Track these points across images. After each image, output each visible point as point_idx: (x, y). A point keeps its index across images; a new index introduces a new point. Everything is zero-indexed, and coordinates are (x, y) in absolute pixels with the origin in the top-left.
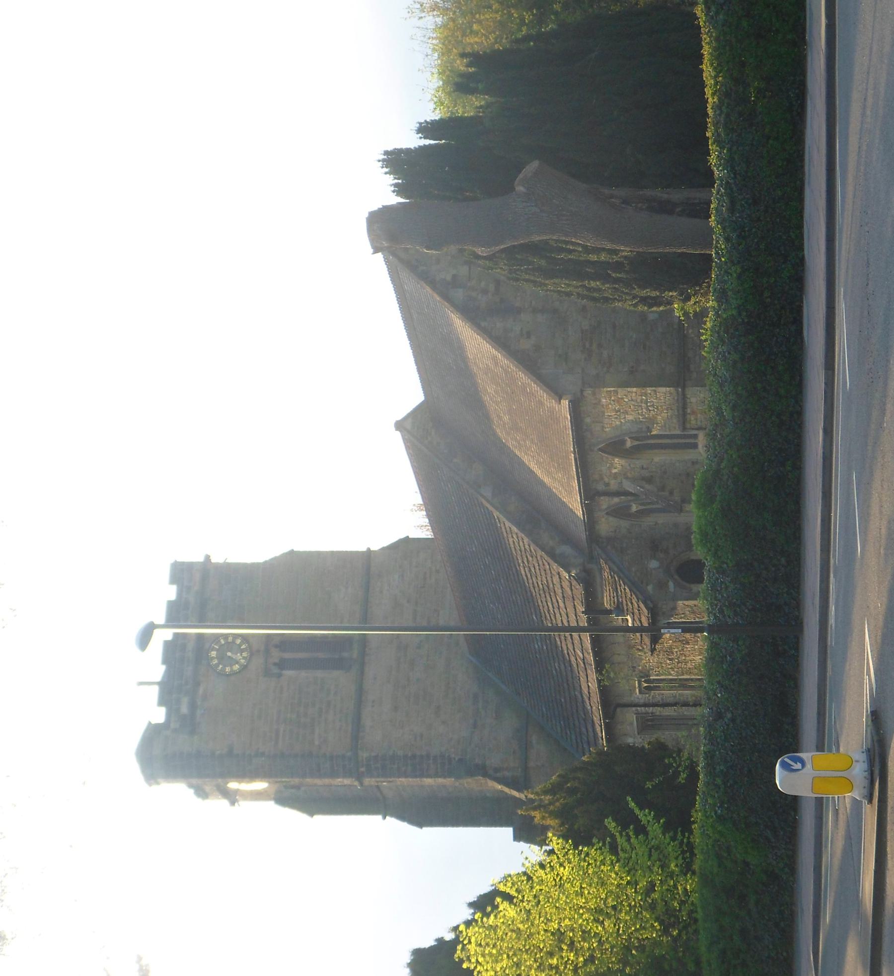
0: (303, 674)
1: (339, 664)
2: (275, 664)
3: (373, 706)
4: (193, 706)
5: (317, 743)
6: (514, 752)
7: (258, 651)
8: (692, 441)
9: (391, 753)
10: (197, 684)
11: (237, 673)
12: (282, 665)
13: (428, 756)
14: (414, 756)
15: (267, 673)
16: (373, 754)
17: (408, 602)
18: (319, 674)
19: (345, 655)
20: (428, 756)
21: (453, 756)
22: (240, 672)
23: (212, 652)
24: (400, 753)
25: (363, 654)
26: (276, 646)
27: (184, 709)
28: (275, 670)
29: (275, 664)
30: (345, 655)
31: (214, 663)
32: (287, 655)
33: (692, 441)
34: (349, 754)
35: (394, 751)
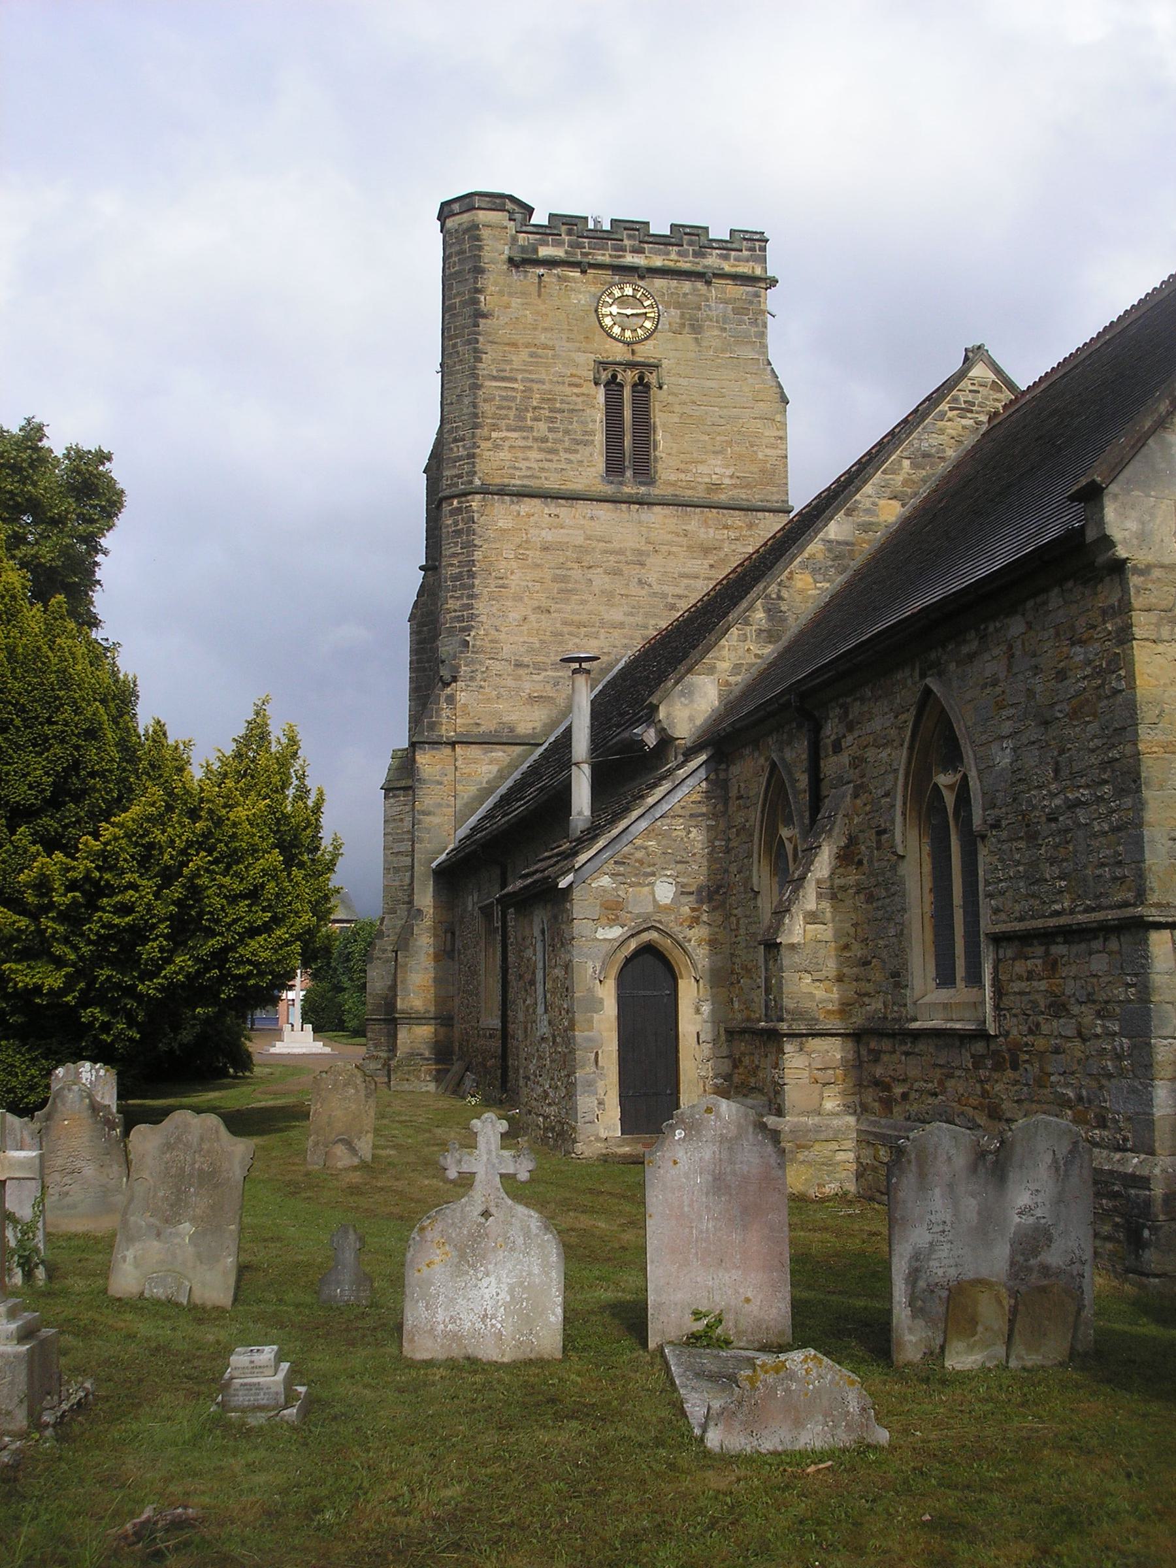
0: (599, 416)
1: (614, 466)
2: (614, 377)
3: (550, 515)
4: (551, 263)
5: (494, 435)
6: (478, 724)
7: (633, 352)
8: (960, 971)
9: (476, 542)
10: (583, 267)
11: (600, 324)
12: (613, 386)
13: (472, 597)
14: (472, 575)
15: (603, 365)
16: (476, 515)
17: (711, 566)
18: (600, 438)
19: (629, 474)
20: (472, 597)
21: (472, 634)
22: (602, 327)
23: (631, 290)
24: (478, 555)
25: (630, 501)
26: (641, 378)
27: (544, 252)
28: (605, 376)
29: (614, 377)
30: (629, 474)
31: (615, 292)
32: (627, 392)
33: (960, 971)
34: (477, 482)
35: (481, 547)
